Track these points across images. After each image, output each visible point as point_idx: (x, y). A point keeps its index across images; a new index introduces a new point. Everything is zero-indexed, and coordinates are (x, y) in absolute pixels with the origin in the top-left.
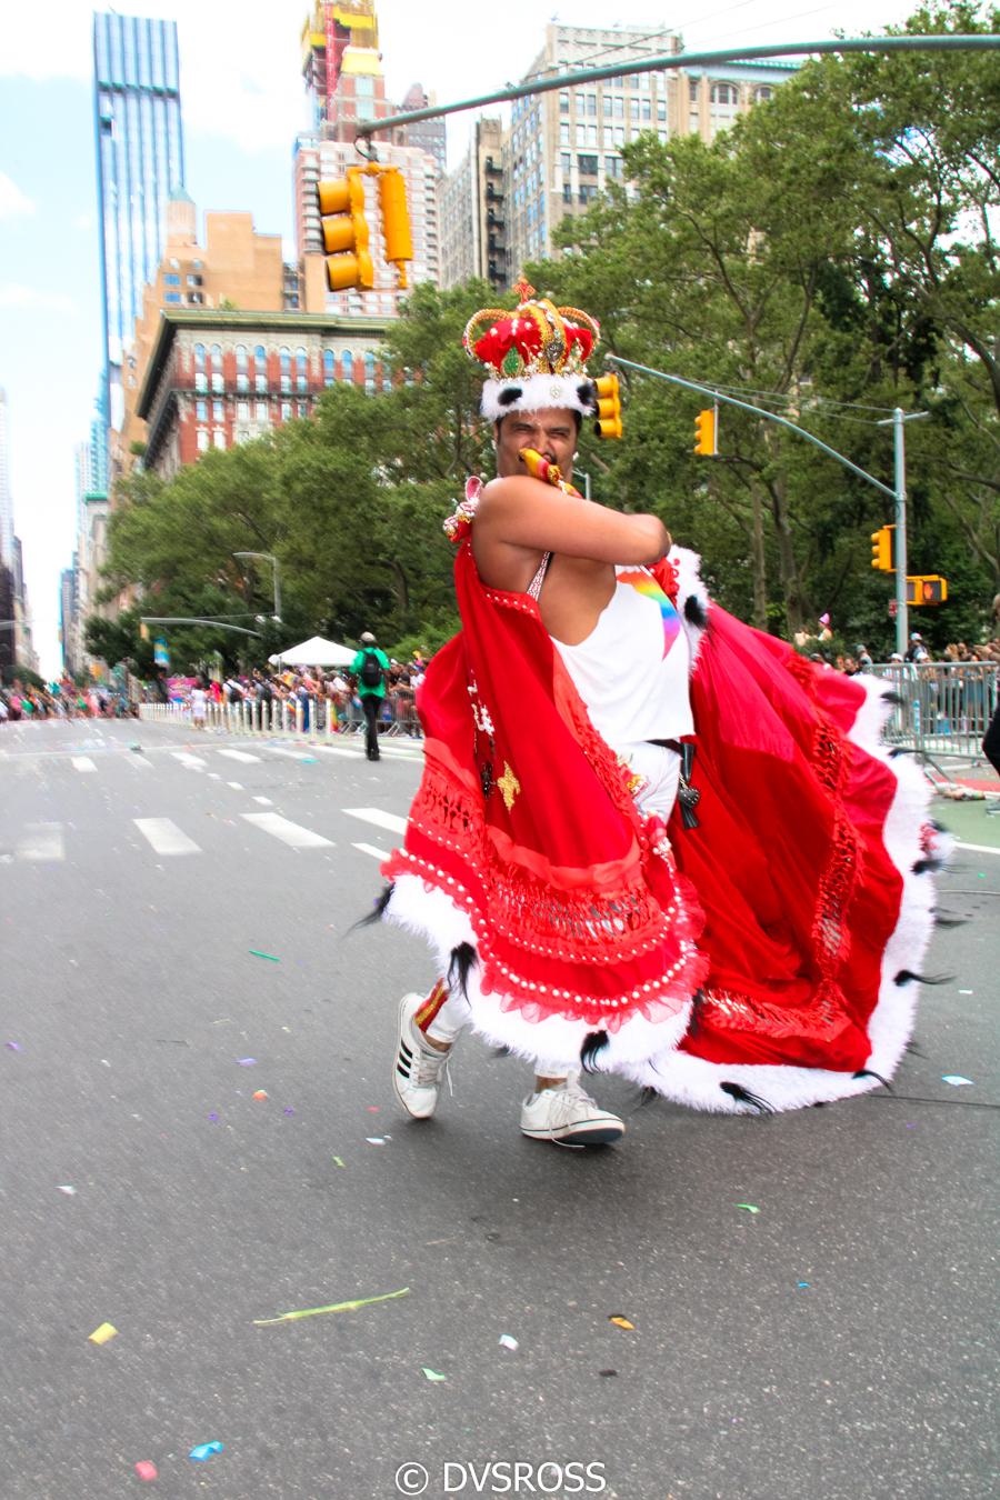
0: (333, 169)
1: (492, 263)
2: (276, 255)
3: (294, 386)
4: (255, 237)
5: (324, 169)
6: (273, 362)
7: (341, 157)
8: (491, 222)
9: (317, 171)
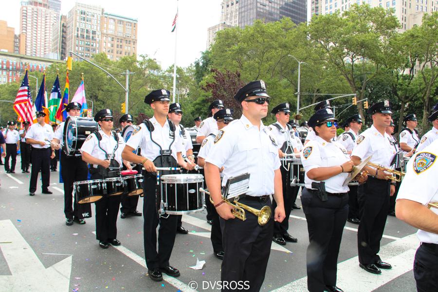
0: (31, 11)
1: (62, 45)
2: (13, 32)
3: (13, 68)
4: (8, 27)
5: (28, 11)
6: (8, 63)
7: (33, 9)
8: (63, 37)
9: (27, 11)
